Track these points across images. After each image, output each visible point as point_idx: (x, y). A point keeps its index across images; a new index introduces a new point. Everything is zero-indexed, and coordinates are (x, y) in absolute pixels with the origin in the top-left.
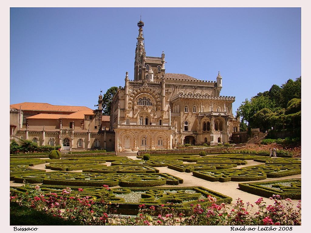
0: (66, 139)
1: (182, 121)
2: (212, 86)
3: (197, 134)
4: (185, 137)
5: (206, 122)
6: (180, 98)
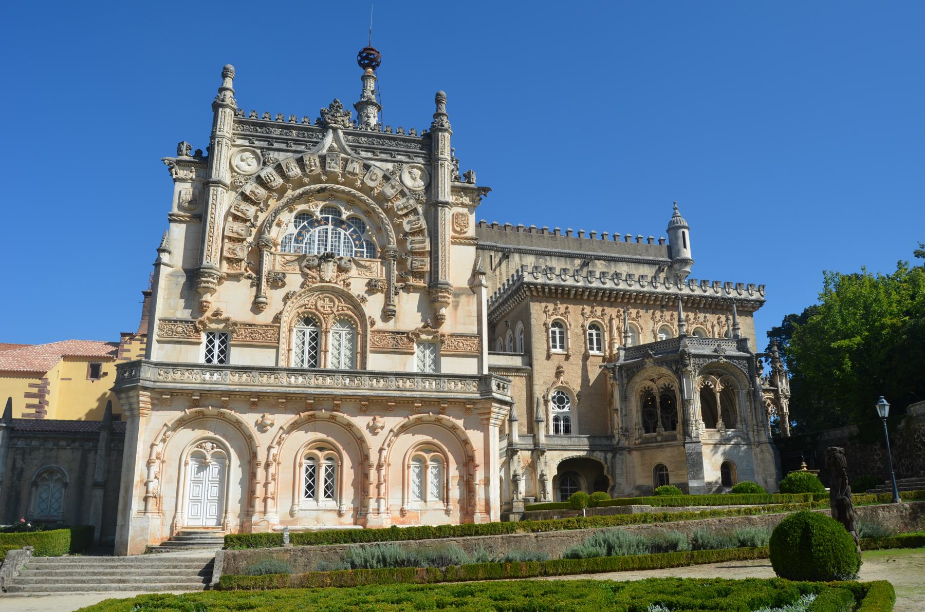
1: (539, 392)
2: (651, 258)
3: (615, 450)
4: (564, 466)
5: (656, 391)
6: (528, 284)
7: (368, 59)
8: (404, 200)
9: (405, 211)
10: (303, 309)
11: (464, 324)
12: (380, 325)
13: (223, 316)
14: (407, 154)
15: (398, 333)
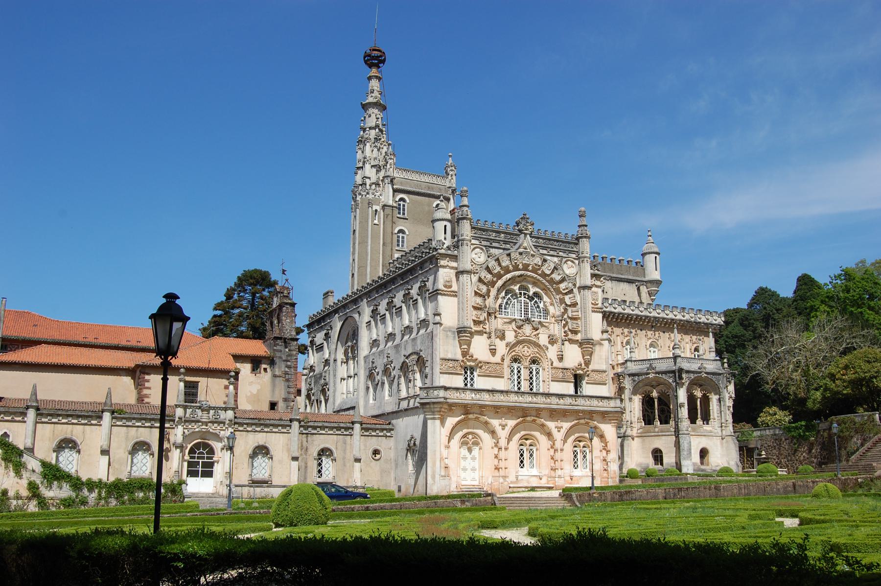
0: (197, 446)
2: (630, 277)
7: (375, 60)
12: (556, 364)
13: (475, 357)
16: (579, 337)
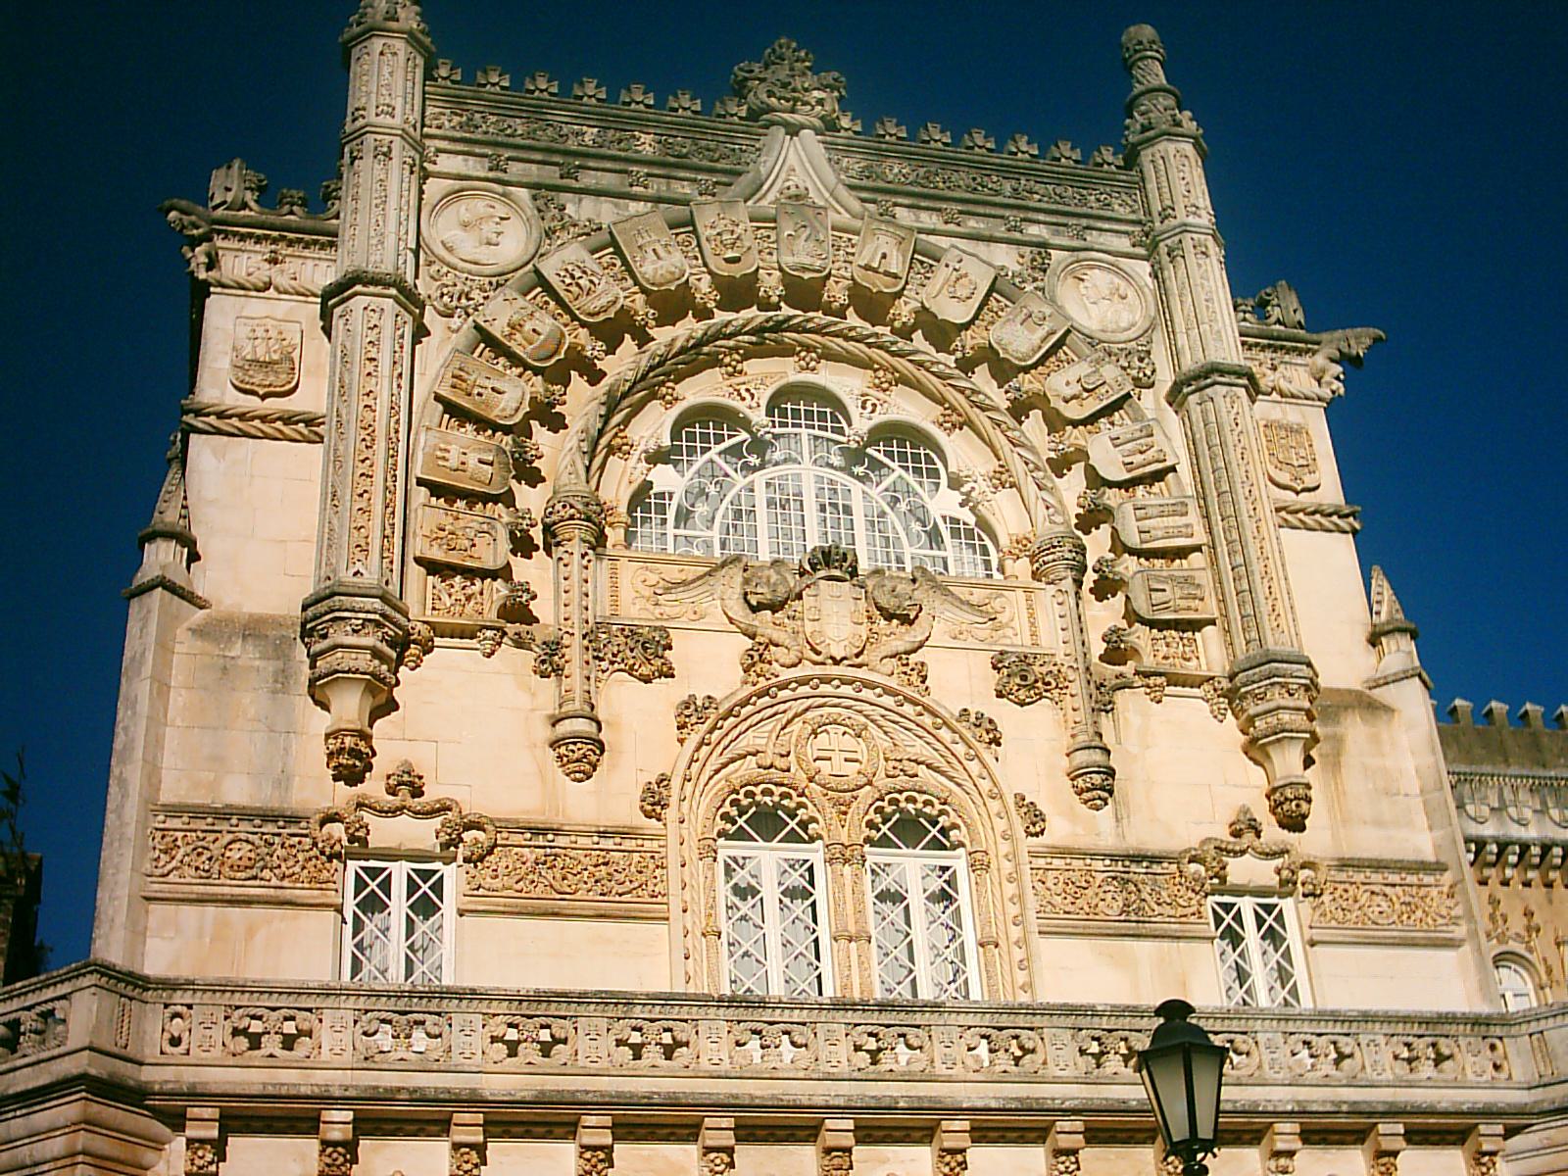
8: (1082, 369)
9: (1092, 405)
10: (748, 768)
11: (1378, 823)
13: (432, 794)
14: (1060, 217)
15: (1137, 858)
16: (1211, 653)
